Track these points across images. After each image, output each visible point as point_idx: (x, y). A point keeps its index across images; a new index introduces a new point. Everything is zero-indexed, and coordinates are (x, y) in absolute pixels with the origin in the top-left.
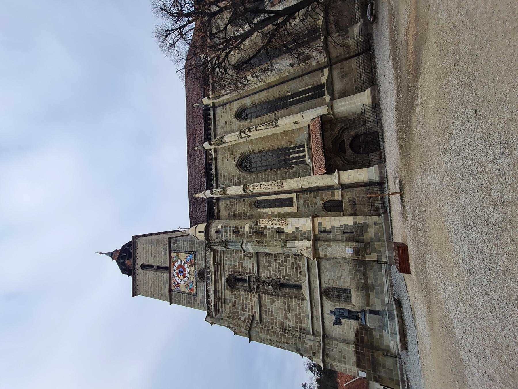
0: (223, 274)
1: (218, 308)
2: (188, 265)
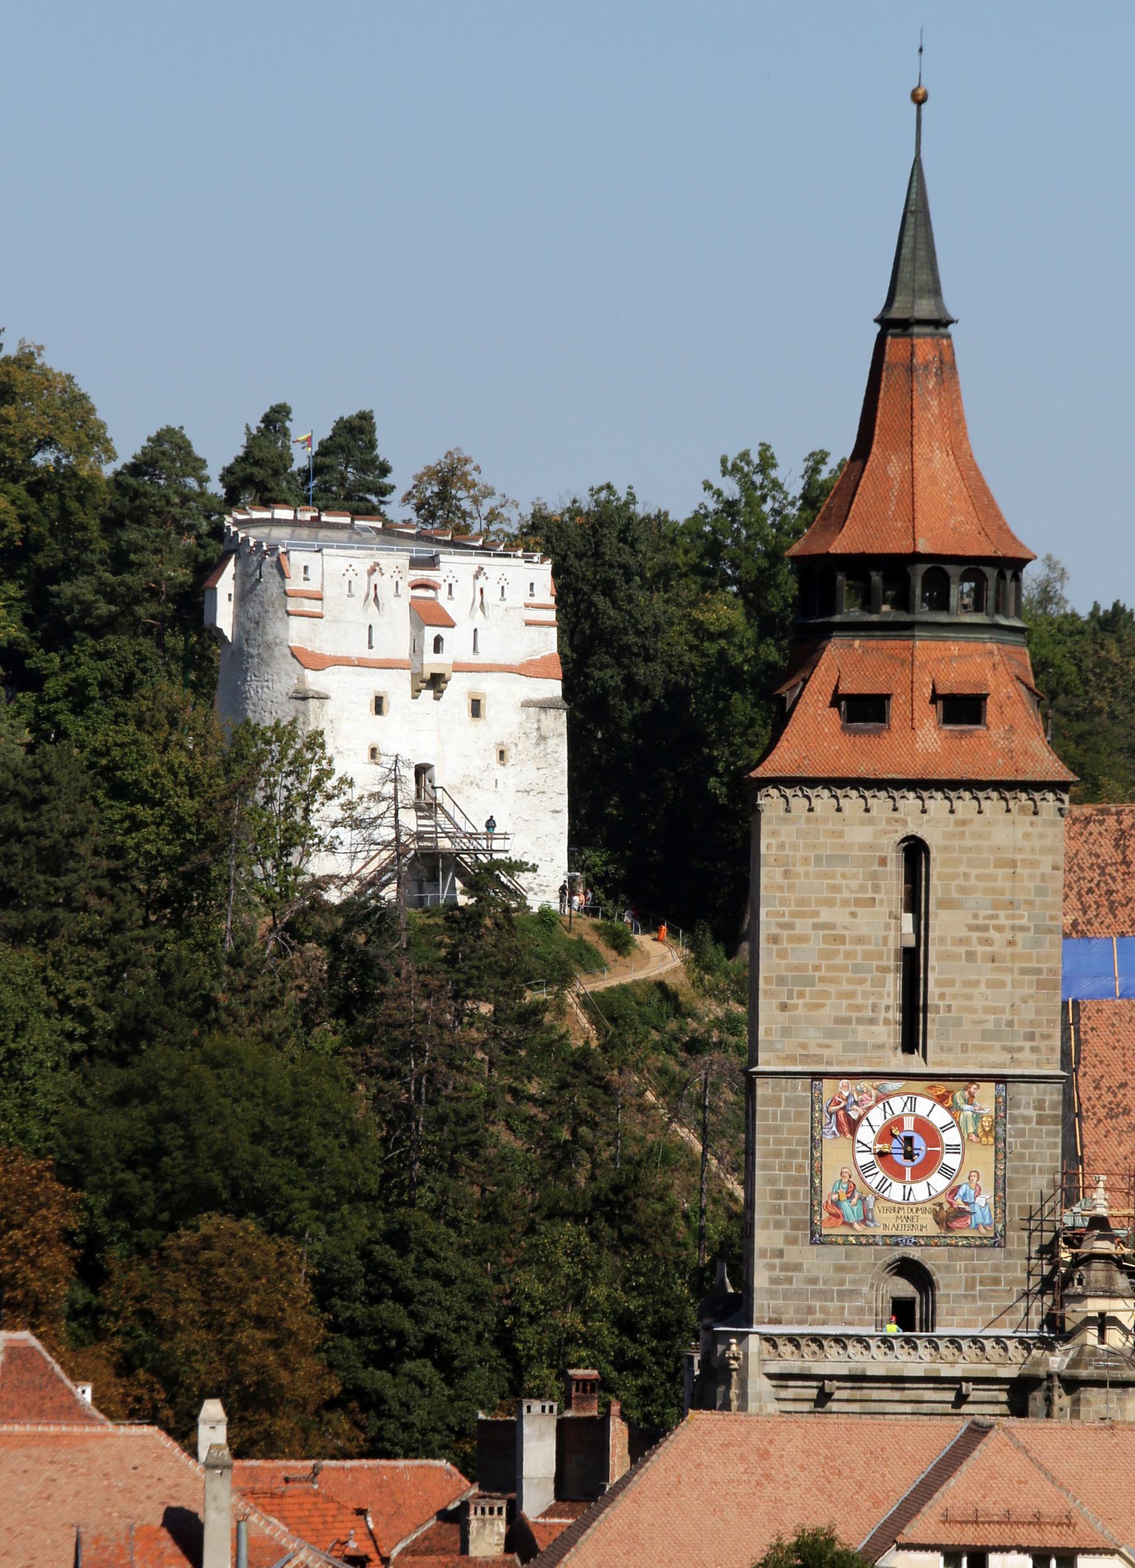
0: (925, 1408)
1: (791, 1383)
2: (942, 1199)
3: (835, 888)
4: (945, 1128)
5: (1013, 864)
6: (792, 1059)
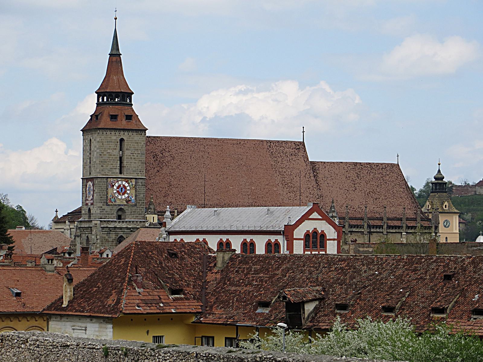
0: (125, 233)
2: (127, 198)
3: (110, 147)
4: (127, 186)
5: (138, 143)
6: (103, 175)
